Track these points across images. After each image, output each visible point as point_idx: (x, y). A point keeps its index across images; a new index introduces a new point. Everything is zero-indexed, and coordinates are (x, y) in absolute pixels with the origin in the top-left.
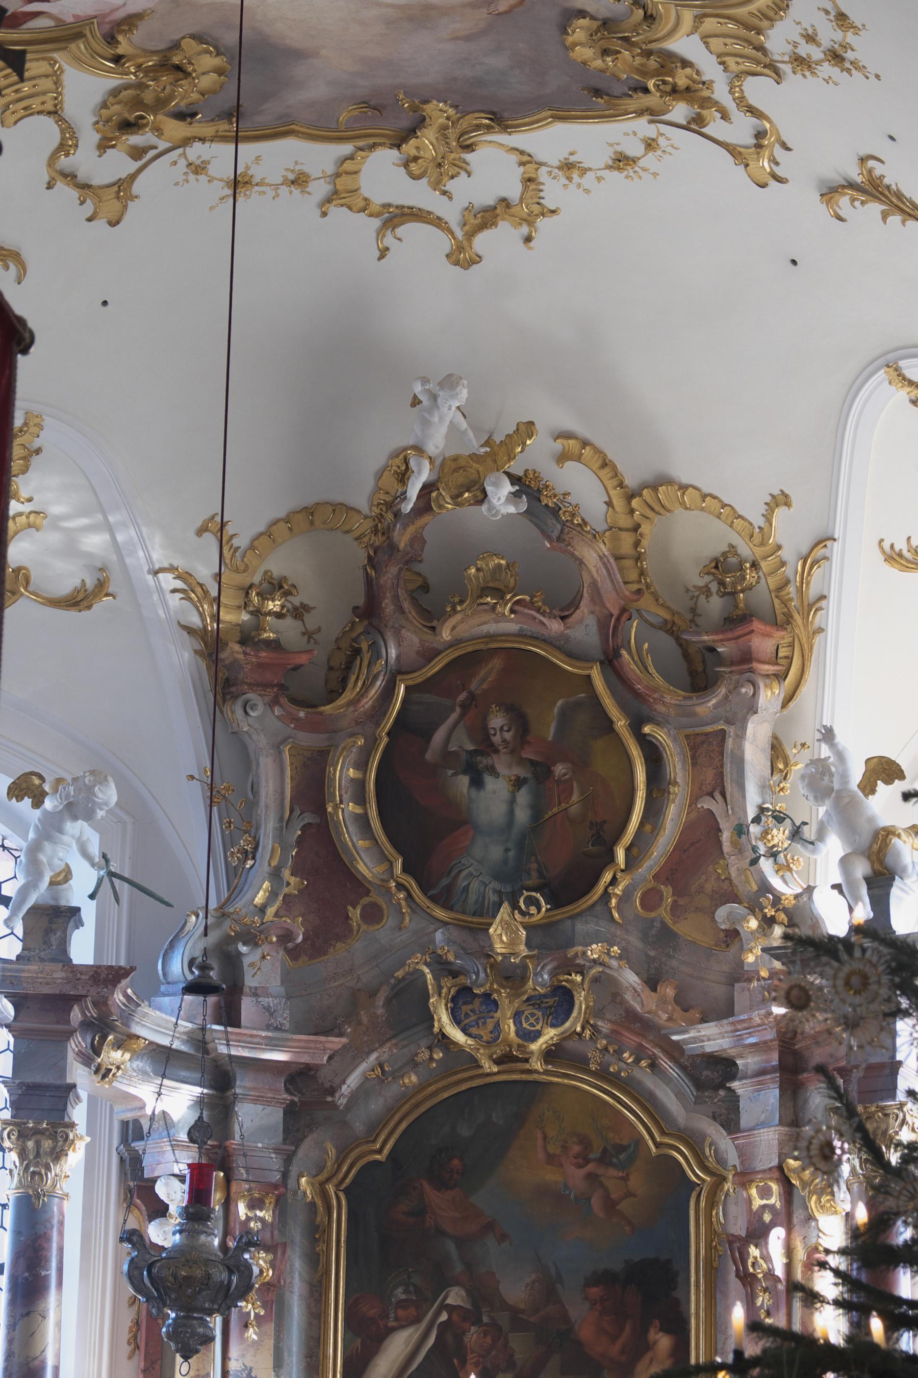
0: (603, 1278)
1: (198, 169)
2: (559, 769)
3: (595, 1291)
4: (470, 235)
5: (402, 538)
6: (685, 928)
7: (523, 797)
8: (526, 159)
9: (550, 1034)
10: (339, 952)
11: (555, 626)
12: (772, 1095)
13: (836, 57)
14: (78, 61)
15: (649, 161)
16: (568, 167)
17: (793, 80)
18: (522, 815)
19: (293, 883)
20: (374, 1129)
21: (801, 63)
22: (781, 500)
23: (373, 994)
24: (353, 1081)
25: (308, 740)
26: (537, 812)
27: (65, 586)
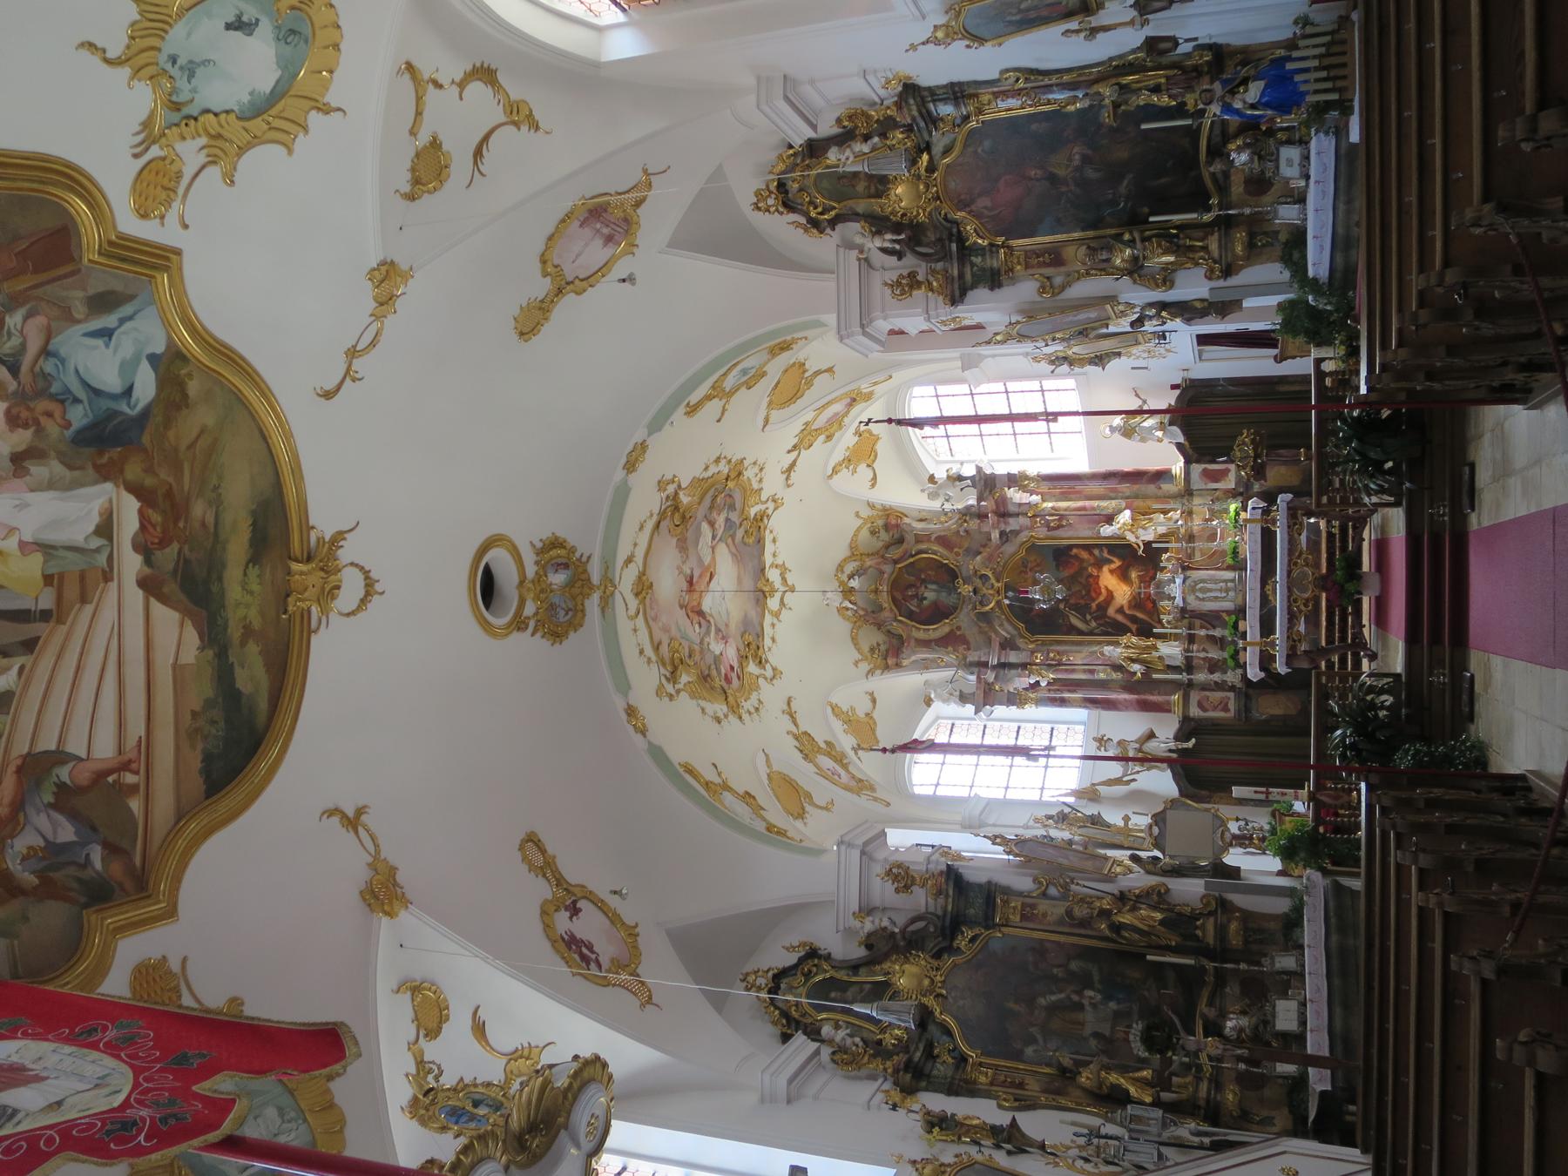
0: (1057, 566)
1: (770, 649)
2: (923, 576)
3: (1061, 569)
4: (787, 585)
5: (862, 613)
6: (966, 545)
7: (930, 586)
8: (771, 566)
9: (993, 580)
10: (971, 640)
11: (886, 575)
12: (1011, 520)
13: (761, 470)
14: (747, 666)
15: (775, 533)
16: (774, 555)
17: (764, 485)
18: (934, 587)
19: (950, 649)
20: (1016, 628)
21: (761, 481)
22: (857, 515)
23: (980, 627)
24: (1004, 633)
25: (913, 643)
26: (934, 583)
27: (870, 704)
